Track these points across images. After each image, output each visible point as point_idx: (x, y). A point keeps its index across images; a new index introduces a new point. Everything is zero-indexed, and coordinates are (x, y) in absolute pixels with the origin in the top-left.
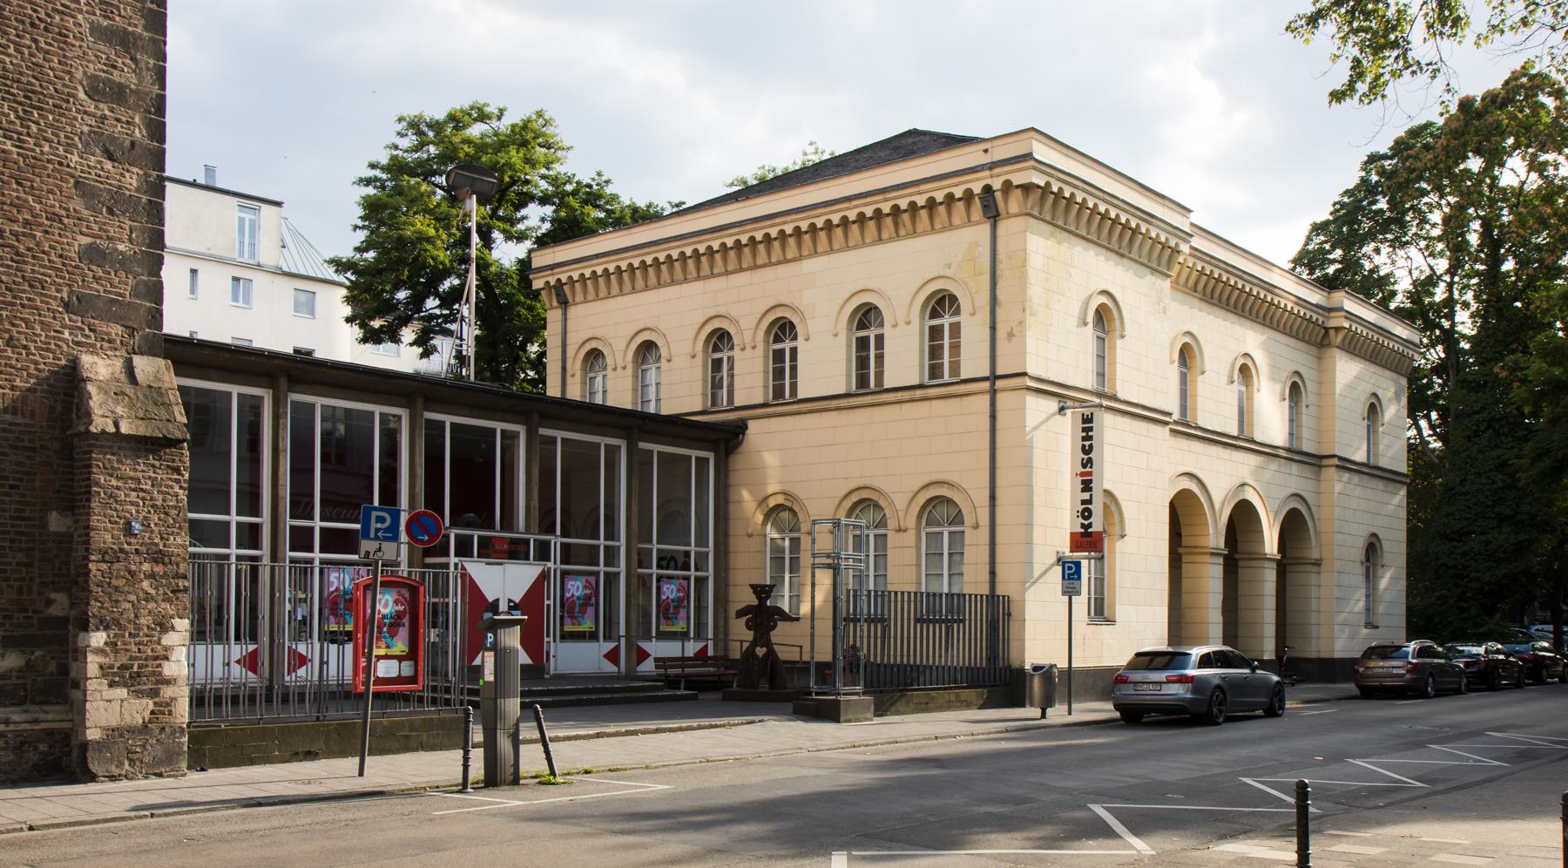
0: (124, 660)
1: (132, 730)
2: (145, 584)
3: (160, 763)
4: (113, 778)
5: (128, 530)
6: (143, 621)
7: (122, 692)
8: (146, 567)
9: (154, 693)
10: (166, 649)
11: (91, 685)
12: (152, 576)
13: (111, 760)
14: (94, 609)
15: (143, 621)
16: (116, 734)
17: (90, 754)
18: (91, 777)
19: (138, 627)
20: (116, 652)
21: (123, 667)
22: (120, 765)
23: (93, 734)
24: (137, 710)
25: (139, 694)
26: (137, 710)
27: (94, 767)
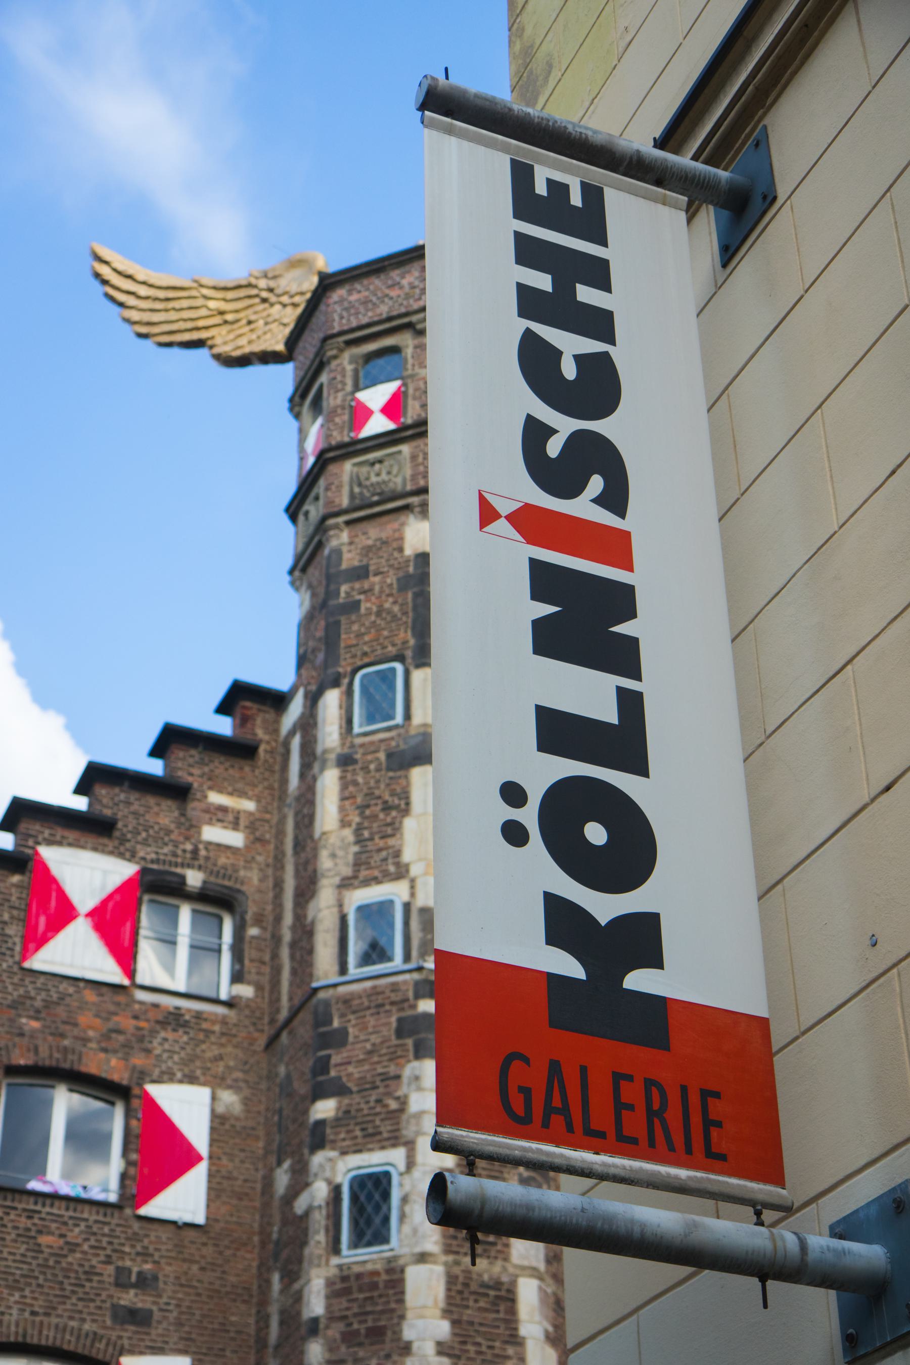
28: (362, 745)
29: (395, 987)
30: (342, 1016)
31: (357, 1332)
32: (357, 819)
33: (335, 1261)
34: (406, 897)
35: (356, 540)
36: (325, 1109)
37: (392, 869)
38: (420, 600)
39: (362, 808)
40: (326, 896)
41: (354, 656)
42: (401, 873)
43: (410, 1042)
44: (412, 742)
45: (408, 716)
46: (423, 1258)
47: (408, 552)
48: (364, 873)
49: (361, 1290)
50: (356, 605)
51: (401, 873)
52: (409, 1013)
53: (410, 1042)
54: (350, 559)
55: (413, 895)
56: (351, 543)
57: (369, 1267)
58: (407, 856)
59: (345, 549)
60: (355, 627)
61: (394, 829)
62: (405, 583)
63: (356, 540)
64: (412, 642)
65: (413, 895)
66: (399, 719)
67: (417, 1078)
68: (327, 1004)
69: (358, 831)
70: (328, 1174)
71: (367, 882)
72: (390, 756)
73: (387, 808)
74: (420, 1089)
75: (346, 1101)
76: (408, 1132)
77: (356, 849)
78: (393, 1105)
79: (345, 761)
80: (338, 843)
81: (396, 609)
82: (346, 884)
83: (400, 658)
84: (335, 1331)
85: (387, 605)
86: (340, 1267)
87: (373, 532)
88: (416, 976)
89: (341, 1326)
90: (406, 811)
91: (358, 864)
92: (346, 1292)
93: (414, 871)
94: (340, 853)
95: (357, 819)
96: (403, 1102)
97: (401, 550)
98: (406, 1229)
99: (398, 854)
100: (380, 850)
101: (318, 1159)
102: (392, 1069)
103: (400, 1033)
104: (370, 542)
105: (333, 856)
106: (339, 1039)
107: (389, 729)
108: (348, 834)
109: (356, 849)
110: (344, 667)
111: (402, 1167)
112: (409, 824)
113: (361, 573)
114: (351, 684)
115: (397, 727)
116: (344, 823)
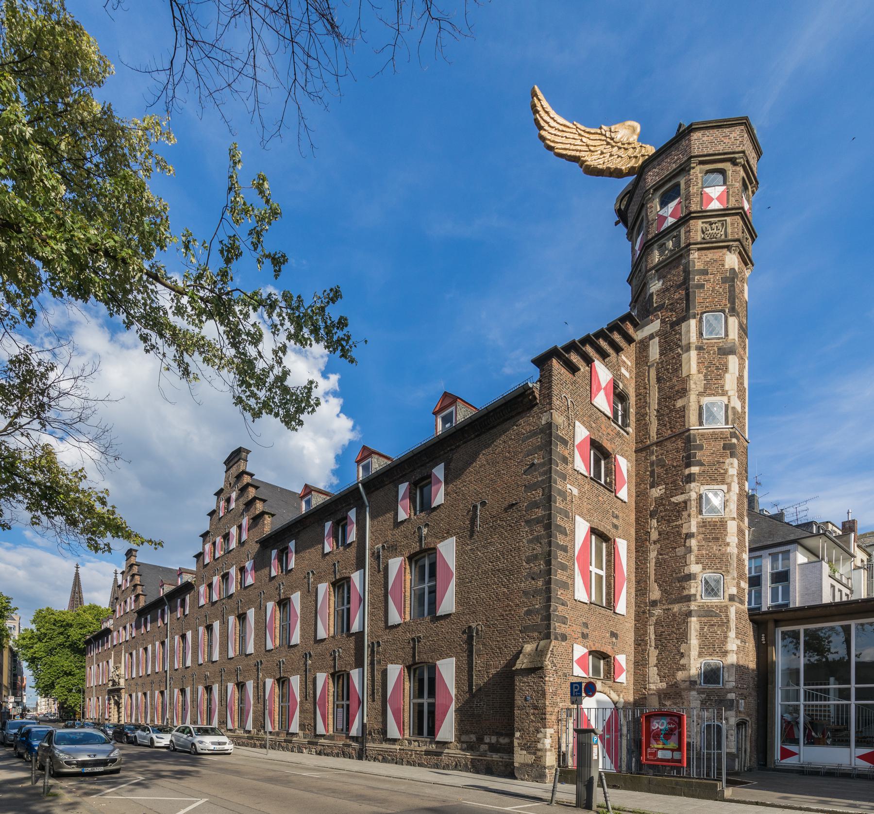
0: (525, 742)
1: (528, 765)
2: (532, 717)
3: (537, 778)
4: (522, 780)
5: (526, 700)
6: (531, 729)
7: (525, 752)
8: (532, 711)
9: (535, 754)
10: (539, 739)
11: (515, 749)
12: (533, 714)
13: (521, 774)
14: (516, 725)
15: (531, 729)
16: (524, 765)
17: (515, 771)
18: (515, 778)
19: (529, 731)
20: (523, 739)
21: (525, 744)
22: (524, 776)
23: (516, 765)
24: (530, 759)
25: (530, 753)
26: (530, 759)
27: (516, 775)
28: (706, 343)
29: (722, 433)
30: (700, 440)
31: (709, 538)
32: (705, 371)
33: (700, 517)
34: (726, 402)
35: (702, 257)
36: (695, 469)
37: (720, 392)
38: (732, 288)
39: (707, 368)
40: (693, 397)
41: (702, 307)
42: (724, 393)
43: (728, 452)
44: (729, 345)
45: (727, 335)
46: (734, 519)
47: (727, 267)
48: (708, 391)
49: (710, 526)
50: (702, 286)
51: (724, 393)
52: (728, 442)
53: (728, 452)
54: (699, 265)
55: (729, 402)
56: (699, 258)
57: (714, 520)
58: (727, 388)
59: (696, 261)
60: (702, 295)
61: (721, 377)
62: (725, 280)
63: (702, 257)
64: (729, 305)
65: (729, 402)
66: (723, 336)
67: (732, 464)
68: (694, 435)
69: (706, 376)
70: (697, 490)
71: (710, 395)
72: (719, 349)
73: (718, 369)
74: (733, 467)
75: (703, 468)
76: (728, 481)
77: (705, 382)
78: (722, 471)
79: (699, 348)
80: (697, 379)
81: (721, 290)
82: (700, 394)
83: (723, 311)
84: (701, 537)
85: (717, 288)
86: (703, 519)
87: (710, 255)
88: (731, 430)
89: (703, 536)
90: (726, 370)
91: (705, 388)
92: (705, 526)
93: (730, 393)
94: (698, 383)
95: (705, 371)
96: (726, 471)
97: (723, 265)
98: (727, 510)
99: (723, 386)
100: (714, 384)
101: (693, 485)
102: (721, 460)
103: (724, 448)
104: (708, 260)
105: (695, 383)
106: (700, 447)
107: (719, 339)
108: (701, 376)
109: (705, 382)
110: (698, 310)
111: (726, 491)
112: (727, 376)
113: (704, 272)
114: (701, 318)
115: (722, 338)
116: (699, 372)
